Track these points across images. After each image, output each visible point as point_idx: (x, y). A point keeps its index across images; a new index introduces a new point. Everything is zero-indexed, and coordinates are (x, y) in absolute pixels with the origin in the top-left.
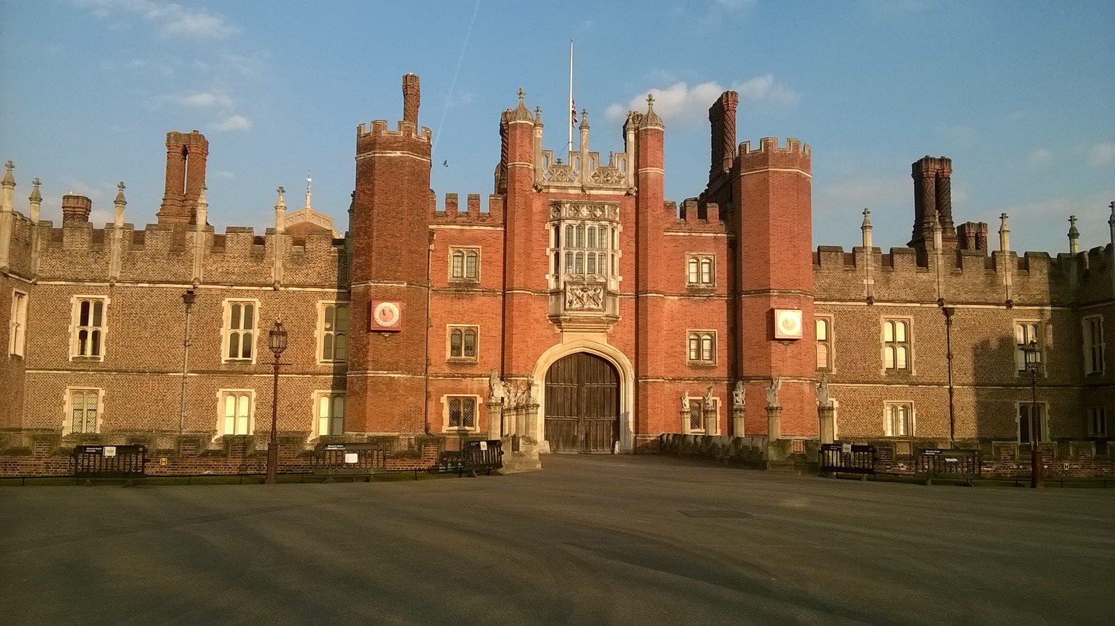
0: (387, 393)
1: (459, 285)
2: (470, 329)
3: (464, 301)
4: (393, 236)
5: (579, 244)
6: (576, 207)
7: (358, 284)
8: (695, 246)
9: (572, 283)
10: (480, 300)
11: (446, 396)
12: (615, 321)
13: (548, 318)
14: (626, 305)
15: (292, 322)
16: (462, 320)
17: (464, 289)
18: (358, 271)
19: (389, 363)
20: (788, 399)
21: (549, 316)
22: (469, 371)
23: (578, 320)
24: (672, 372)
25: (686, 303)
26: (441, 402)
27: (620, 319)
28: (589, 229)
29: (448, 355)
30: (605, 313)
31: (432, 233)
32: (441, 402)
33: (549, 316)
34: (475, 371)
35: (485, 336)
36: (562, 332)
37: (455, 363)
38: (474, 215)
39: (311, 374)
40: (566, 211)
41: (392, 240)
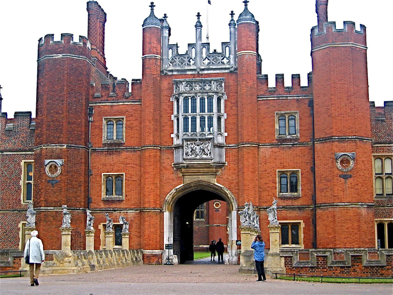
0: (54, 223)
1: (111, 145)
2: (117, 176)
3: (114, 156)
4: (57, 113)
5: (194, 110)
6: (189, 83)
7: (37, 148)
8: (282, 107)
9: (187, 140)
10: (124, 154)
11: (102, 224)
12: (222, 166)
13: (173, 166)
14: (231, 154)
15: (6, 176)
16: (113, 170)
17: (114, 148)
18: (37, 139)
19: (55, 202)
20: (347, 220)
21: (174, 165)
22: (118, 207)
23: (193, 166)
24: (266, 202)
25: (276, 150)
26: (99, 228)
27: (227, 164)
28: (200, 99)
29: (104, 196)
30: (213, 160)
32: (99, 228)
33: (174, 165)
34: (122, 206)
35: (128, 180)
36: (183, 175)
37: (108, 201)
38: (120, 95)
39: (18, 211)
40: (182, 88)
41: (56, 116)
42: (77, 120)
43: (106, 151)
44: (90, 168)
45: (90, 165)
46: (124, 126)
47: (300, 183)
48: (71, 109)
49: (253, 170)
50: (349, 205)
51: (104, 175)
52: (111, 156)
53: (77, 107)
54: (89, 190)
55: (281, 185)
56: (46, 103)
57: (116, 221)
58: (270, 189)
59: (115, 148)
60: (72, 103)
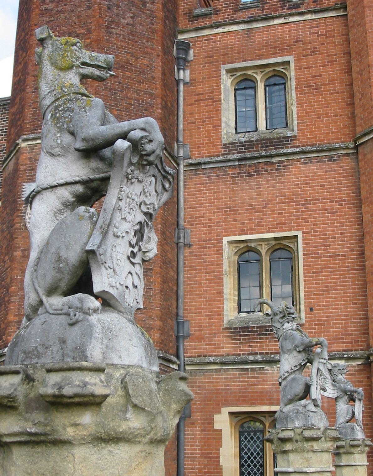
1: (250, 145)
3: (263, 180)
16: (260, 224)
31: (185, 47)
35: (316, 256)
42: (137, 58)
43: (234, 167)
44: (181, 222)
45: (182, 214)
46: (292, 84)
48: (118, 24)
51: (230, 242)
52: (254, 180)
53: (138, 20)
54: (181, 293)
56: (37, 11)
57: (278, 399)
59: (264, 153)
60: (118, 6)
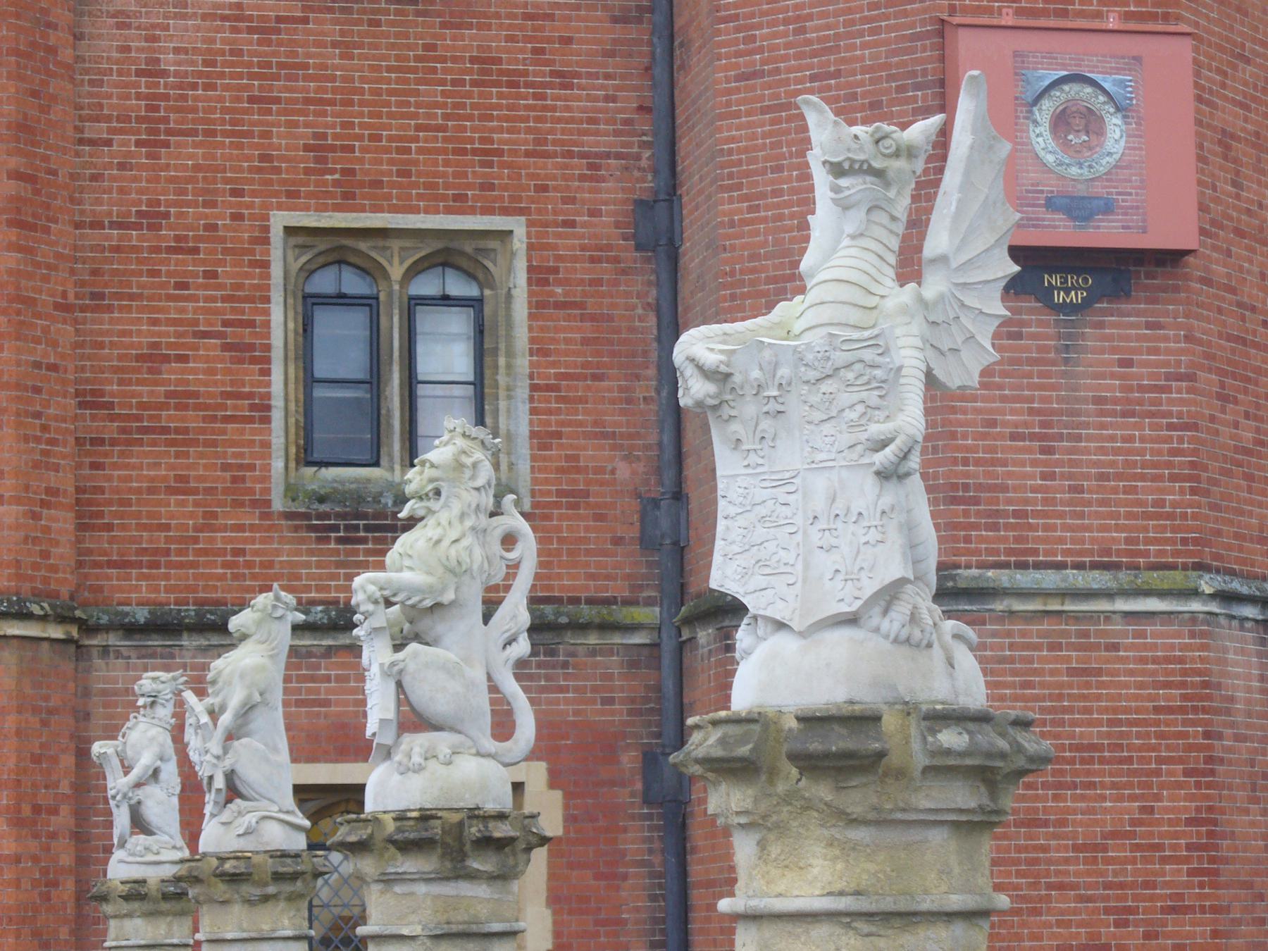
47: (523, 363)
49: (25, 190)
50: (1109, 595)
55: (309, 380)
58: (193, 420)
